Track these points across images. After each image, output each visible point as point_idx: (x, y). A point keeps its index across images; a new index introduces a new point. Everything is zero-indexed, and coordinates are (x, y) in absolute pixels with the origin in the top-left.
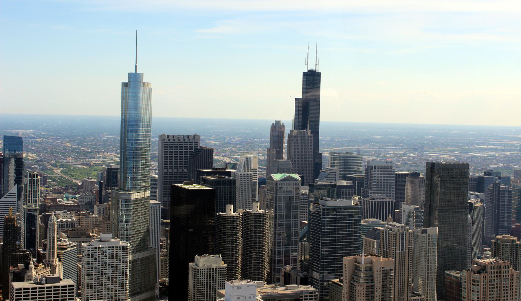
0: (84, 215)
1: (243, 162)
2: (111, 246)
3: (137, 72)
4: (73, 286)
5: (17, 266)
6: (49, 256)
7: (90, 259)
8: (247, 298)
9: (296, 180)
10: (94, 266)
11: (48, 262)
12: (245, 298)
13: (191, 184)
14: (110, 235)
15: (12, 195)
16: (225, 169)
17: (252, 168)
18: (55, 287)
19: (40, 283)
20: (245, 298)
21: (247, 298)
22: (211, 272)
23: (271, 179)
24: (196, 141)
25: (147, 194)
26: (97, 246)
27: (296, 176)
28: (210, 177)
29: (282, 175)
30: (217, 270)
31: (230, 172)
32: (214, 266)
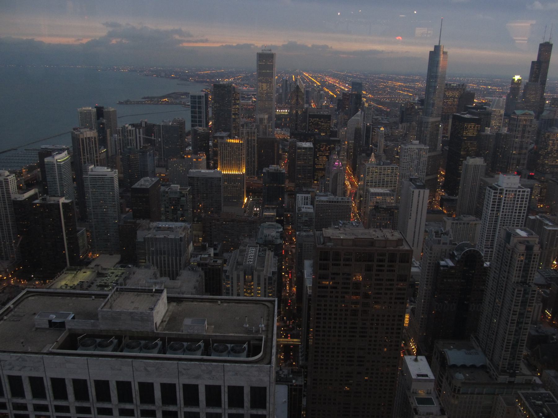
0: (394, 129)
1: (496, 101)
2: (418, 147)
3: (440, 45)
4: (398, 168)
5: (361, 155)
6: (379, 150)
7: (406, 154)
8: (513, 184)
9: (531, 115)
10: (407, 158)
11: (378, 154)
12: (512, 184)
13: (466, 114)
14: (418, 142)
15: (358, 116)
16: (483, 106)
17: (501, 106)
18: (388, 168)
19: (380, 165)
20: (512, 184)
21: (513, 184)
22: (476, 167)
23: (514, 113)
24: (464, 87)
25: (439, 119)
26: (411, 147)
27: (532, 113)
28: (475, 111)
29: (522, 111)
30: (480, 166)
31: (486, 108)
32: (478, 164)
